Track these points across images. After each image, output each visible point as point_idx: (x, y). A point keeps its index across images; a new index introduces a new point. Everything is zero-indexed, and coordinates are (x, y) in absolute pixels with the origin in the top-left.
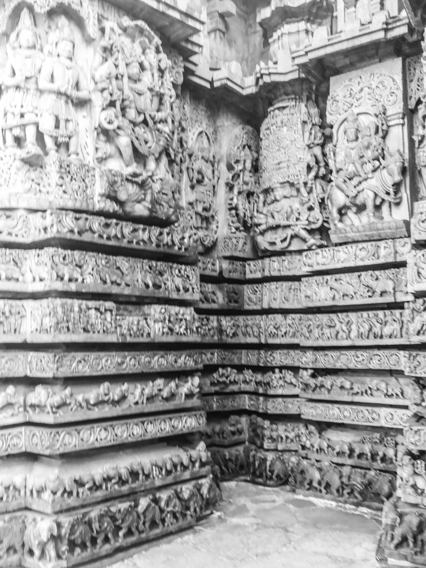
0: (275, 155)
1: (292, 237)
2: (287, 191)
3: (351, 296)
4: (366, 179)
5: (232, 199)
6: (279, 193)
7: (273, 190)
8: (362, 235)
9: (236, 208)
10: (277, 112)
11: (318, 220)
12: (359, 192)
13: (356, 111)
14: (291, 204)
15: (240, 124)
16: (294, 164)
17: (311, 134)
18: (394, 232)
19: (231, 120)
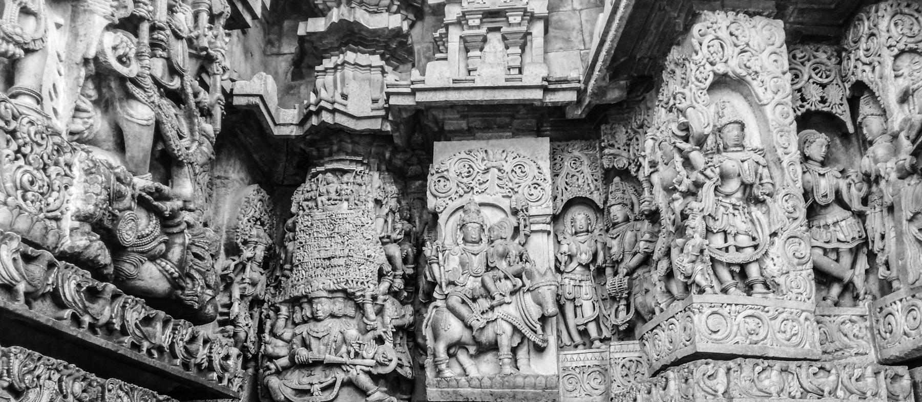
0: (323, 243)
1: (344, 384)
2: (340, 306)
4: (501, 305)
5: (229, 306)
6: (323, 307)
7: (310, 301)
8: (485, 394)
9: (233, 323)
10: (330, 176)
11: (390, 361)
12: (488, 322)
13: (478, 199)
14: (343, 329)
15: (249, 184)
16: (360, 264)
17: (386, 221)
18: (539, 394)
19: (238, 172)
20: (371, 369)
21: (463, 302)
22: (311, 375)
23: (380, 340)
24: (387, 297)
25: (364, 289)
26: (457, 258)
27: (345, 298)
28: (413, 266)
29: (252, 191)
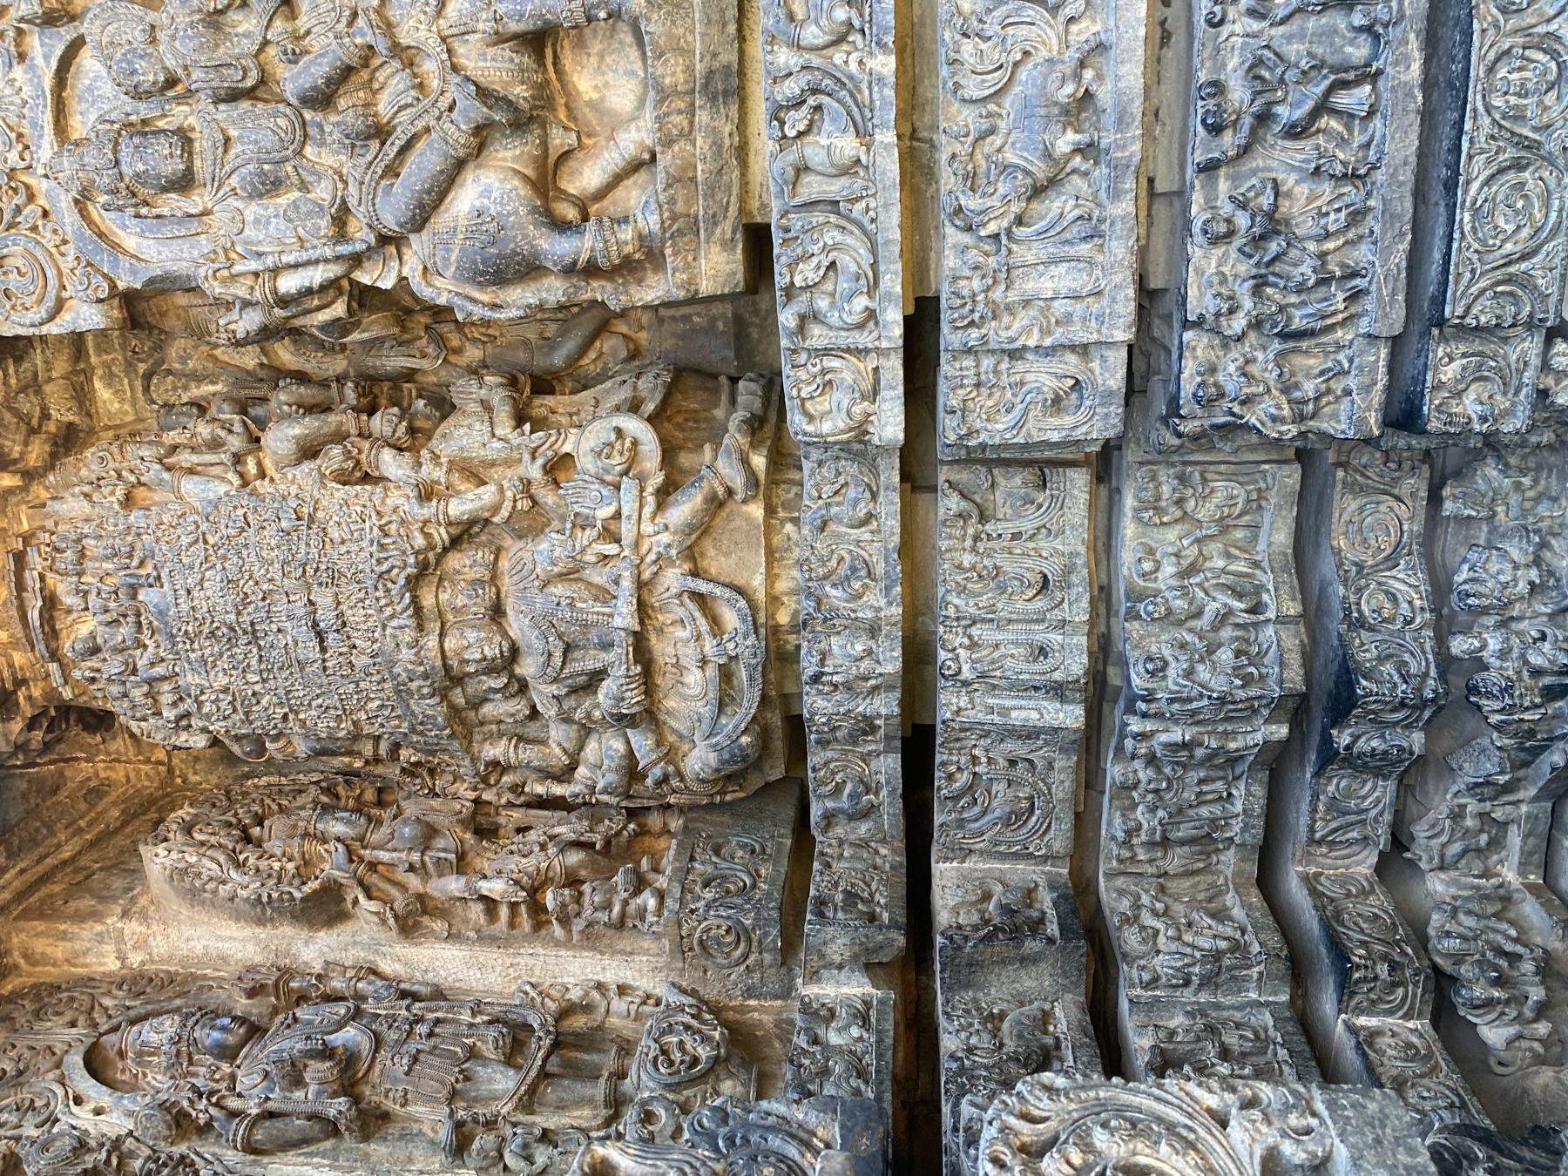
3: (1088, 74)
4: (389, 27)
5: (490, 904)
11: (619, 432)
12: (455, 68)
17: (191, 471)
20: (650, 489)
21: (392, 171)
22: (677, 665)
23: (558, 467)
24: (424, 452)
25: (403, 522)
26: (252, 210)
27: (441, 580)
28: (334, 385)
29: (158, 860)
